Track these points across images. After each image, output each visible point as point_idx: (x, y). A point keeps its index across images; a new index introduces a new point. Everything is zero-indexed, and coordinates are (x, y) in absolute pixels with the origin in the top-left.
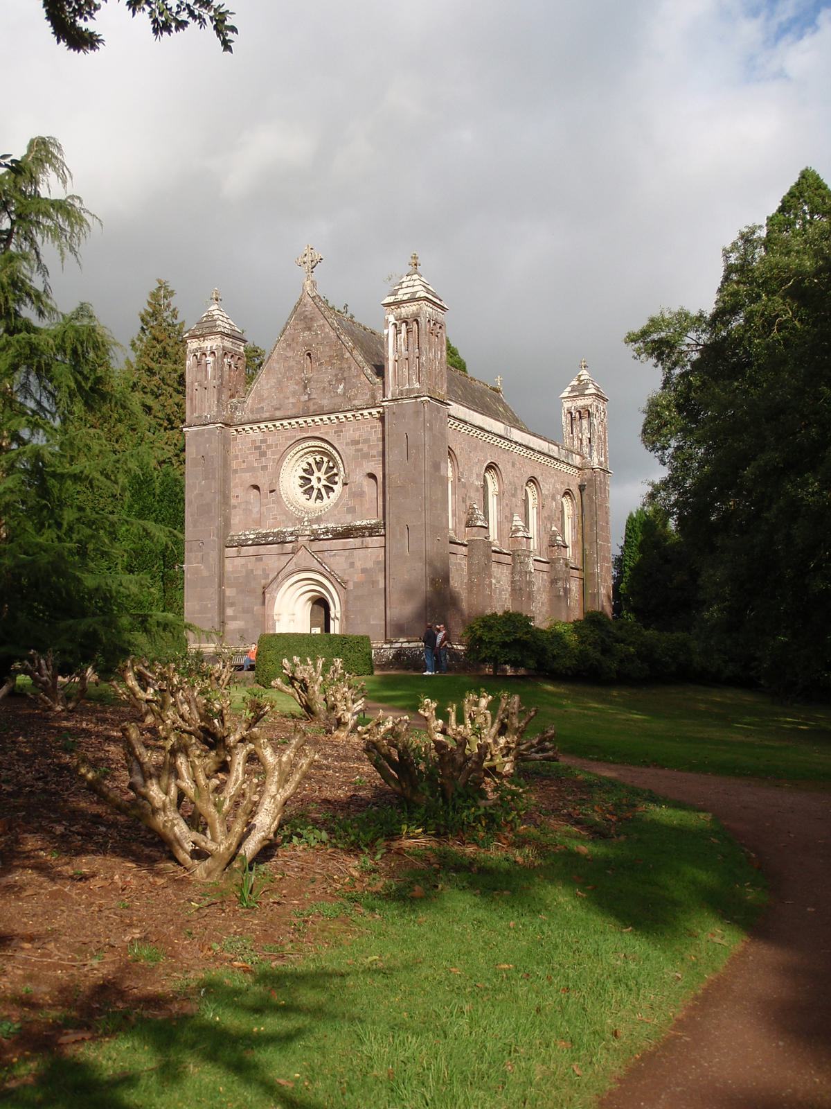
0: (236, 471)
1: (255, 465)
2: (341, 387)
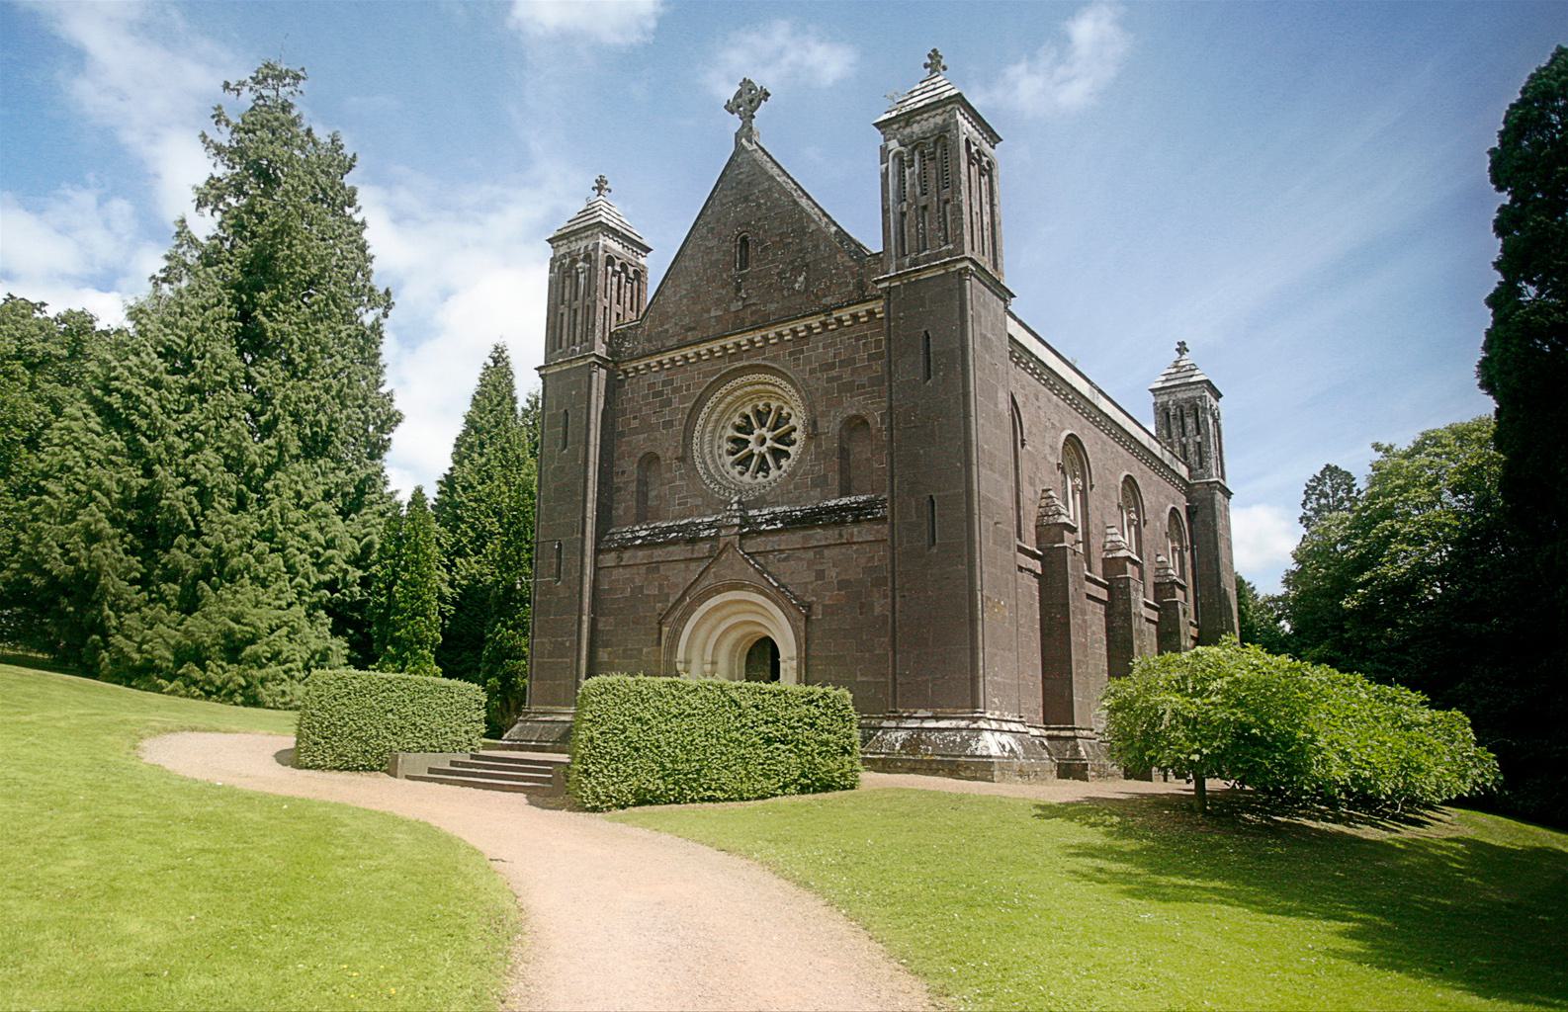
0: (622, 434)
1: (653, 420)
2: (801, 279)
